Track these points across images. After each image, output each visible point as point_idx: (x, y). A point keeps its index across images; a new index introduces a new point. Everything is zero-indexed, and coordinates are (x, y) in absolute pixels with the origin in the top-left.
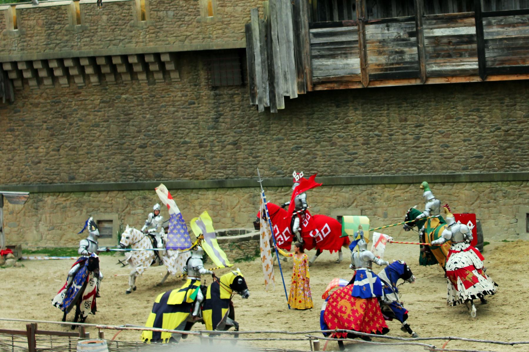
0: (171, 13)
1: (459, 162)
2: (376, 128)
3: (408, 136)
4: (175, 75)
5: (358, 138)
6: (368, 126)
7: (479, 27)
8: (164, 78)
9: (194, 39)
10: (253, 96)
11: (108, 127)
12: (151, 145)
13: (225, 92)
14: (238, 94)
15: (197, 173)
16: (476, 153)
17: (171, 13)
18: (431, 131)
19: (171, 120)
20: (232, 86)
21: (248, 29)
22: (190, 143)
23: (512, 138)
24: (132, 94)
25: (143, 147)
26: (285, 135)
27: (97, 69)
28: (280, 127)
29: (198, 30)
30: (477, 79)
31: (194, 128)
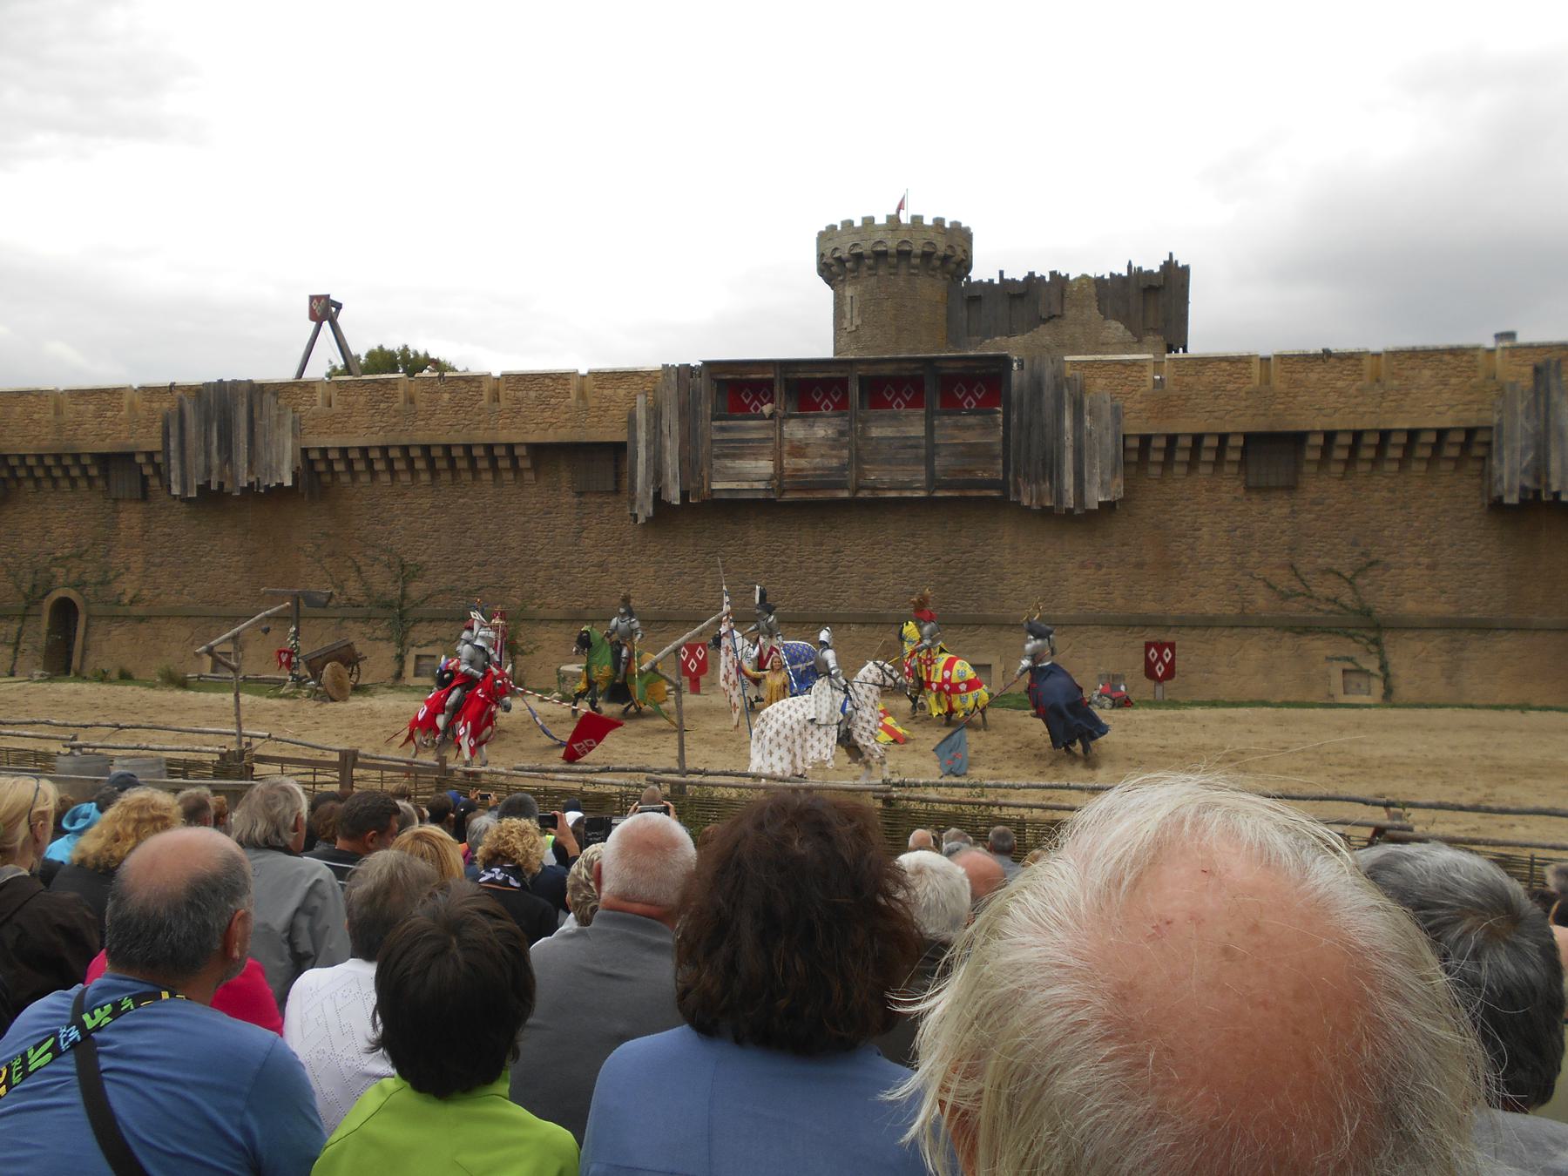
0: (532, 394)
1: (884, 599)
2: (783, 552)
3: (822, 564)
4: (529, 476)
5: (759, 564)
6: (773, 550)
7: (930, 429)
8: (515, 479)
9: (561, 427)
10: (633, 503)
11: (438, 538)
12: (492, 562)
13: (593, 499)
14: (609, 503)
15: (548, 600)
16: (907, 587)
17: (532, 394)
18: (852, 559)
19: (520, 533)
20: (602, 492)
21: (631, 421)
22: (542, 562)
23: (953, 571)
24: (471, 499)
25: (481, 565)
26: (666, 557)
27: (431, 462)
28: (659, 547)
29: (567, 416)
30: (922, 494)
31: (548, 543)
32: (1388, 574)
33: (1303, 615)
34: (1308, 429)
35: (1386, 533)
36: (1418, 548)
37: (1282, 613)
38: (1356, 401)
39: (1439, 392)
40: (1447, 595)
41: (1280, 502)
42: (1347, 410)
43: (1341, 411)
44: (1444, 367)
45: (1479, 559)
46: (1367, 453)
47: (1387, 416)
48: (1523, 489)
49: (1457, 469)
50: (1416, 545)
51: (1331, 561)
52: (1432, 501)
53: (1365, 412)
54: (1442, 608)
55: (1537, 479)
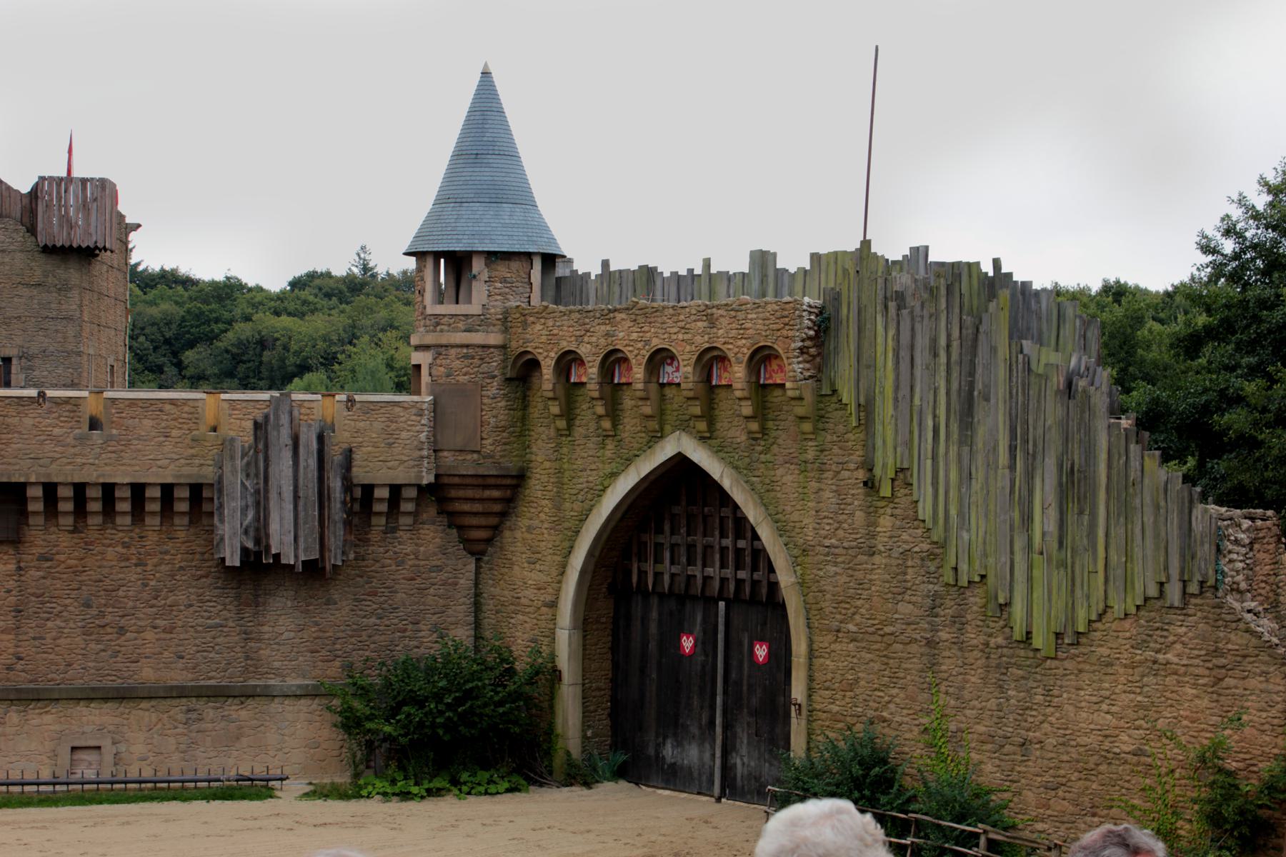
32: (123, 638)
33: (32, 686)
34: (22, 480)
35: (121, 593)
36: (154, 610)
37: (9, 683)
38: (72, 450)
39: (160, 444)
40: (184, 661)
41: (6, 557)
42: (65, 460)
43: (58, 462)
44: (165, 417)
45: (217, 621)
46: (95, 506)
47: (107, 468)
48: (245, 551)
49: (191, 522)
50: (151, 607)
51: (63, 625)
52: (167, 557)
53: (84, 464)
54: (178, 676)
55: (257, 541)
